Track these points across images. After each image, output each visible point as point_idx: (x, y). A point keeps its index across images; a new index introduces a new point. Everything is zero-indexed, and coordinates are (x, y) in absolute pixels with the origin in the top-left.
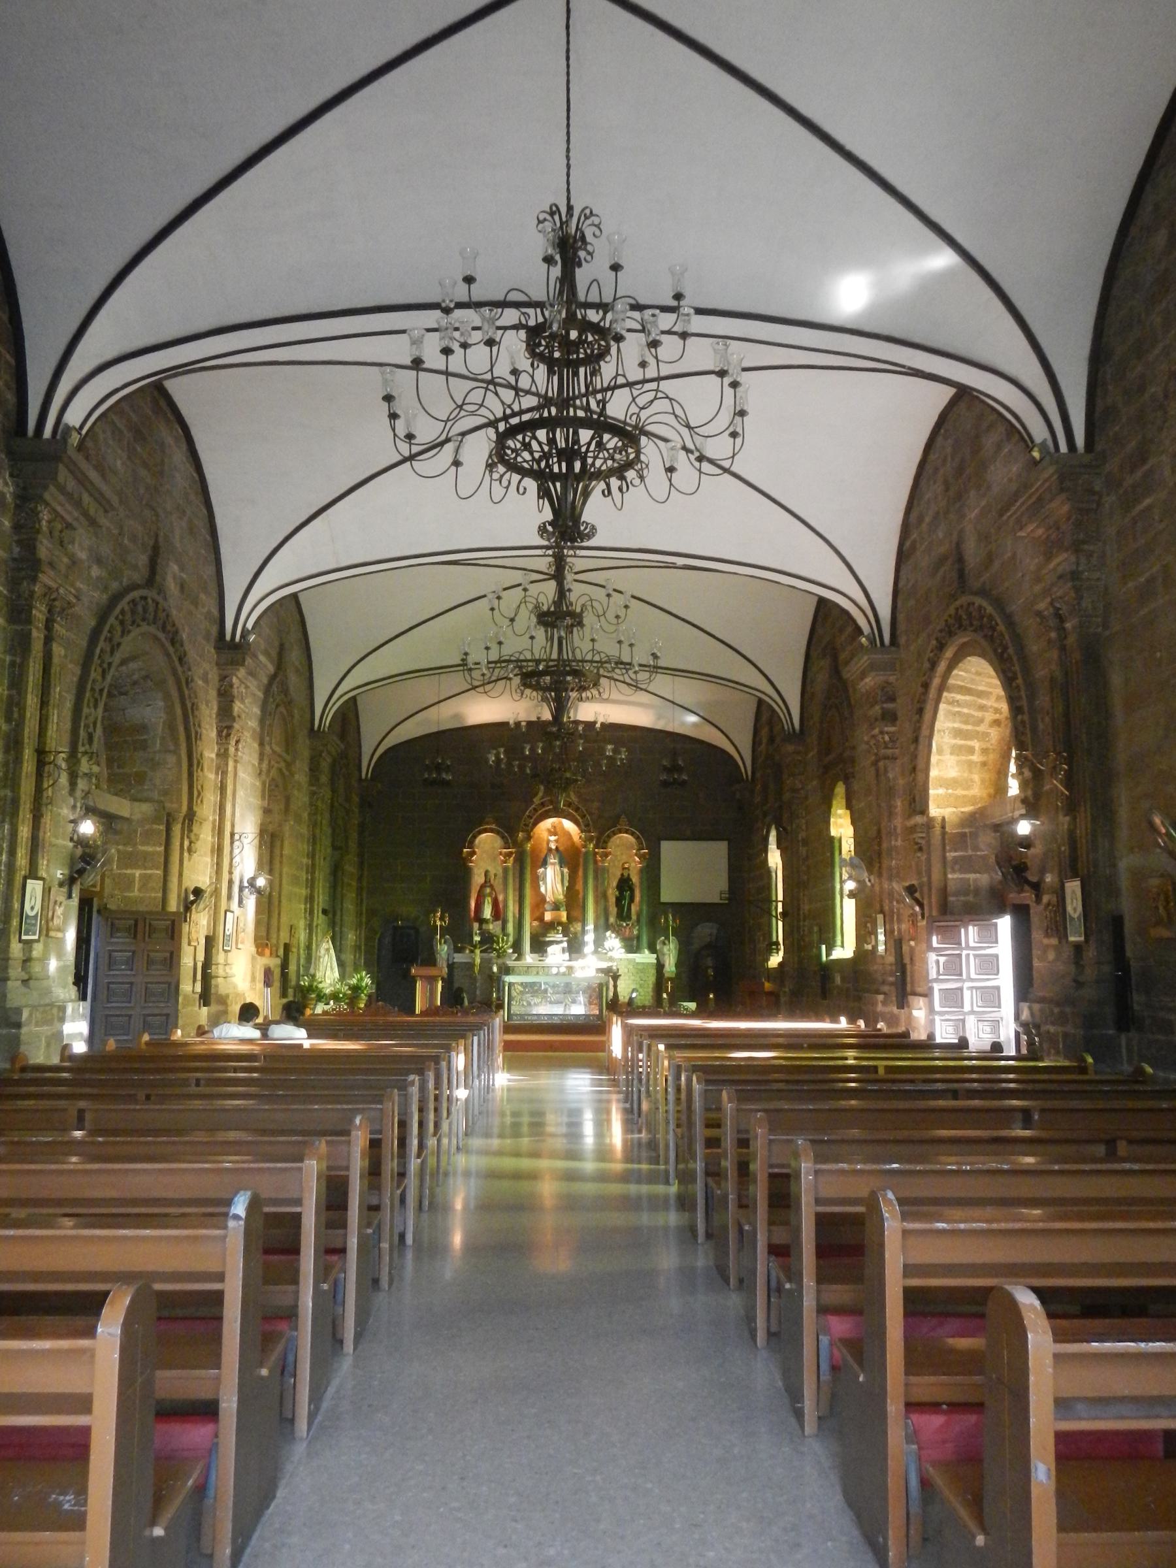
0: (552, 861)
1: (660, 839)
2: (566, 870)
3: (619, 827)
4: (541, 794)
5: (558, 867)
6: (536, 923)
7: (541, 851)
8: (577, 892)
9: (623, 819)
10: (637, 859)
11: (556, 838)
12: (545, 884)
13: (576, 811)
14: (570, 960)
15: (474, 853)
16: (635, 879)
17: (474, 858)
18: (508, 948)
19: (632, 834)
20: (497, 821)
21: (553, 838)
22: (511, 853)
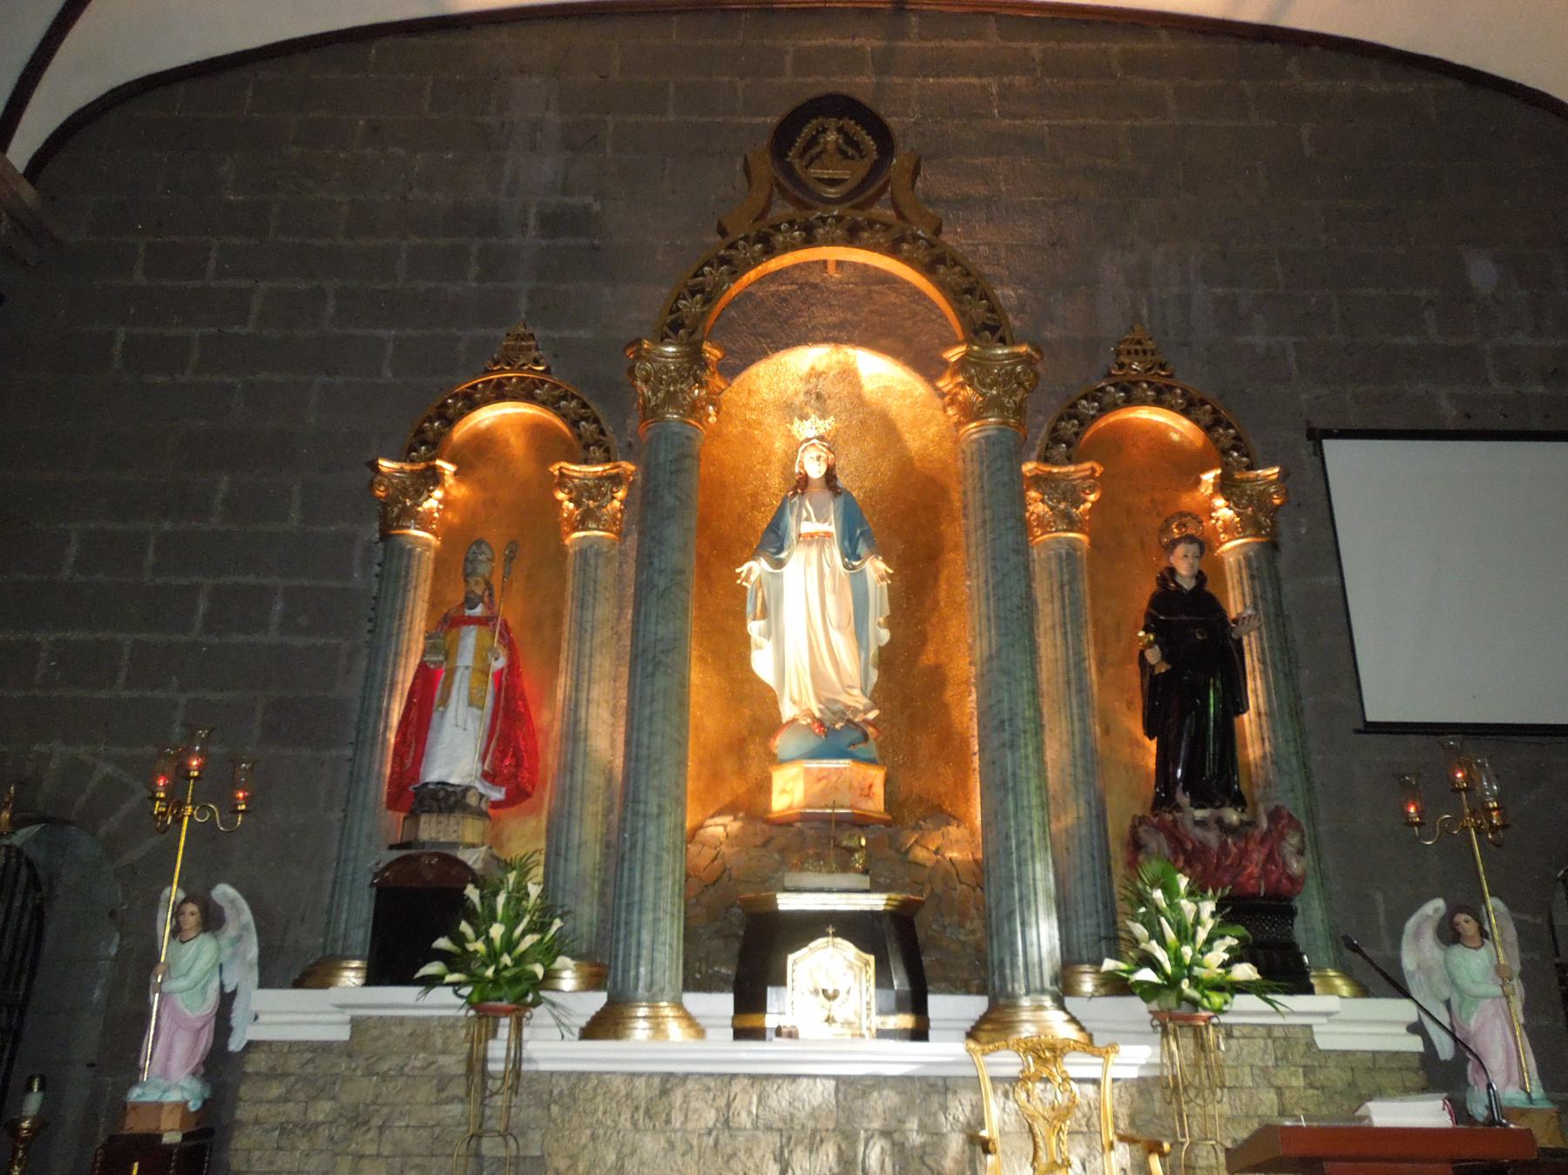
0: (806, 527)
1: (1317, 436)
2: (875, 568)
5: (834, 554)
6: (720, 828)
7: (755, 503)
8: (937, 678)
10: (1224, 511)
11: (825, 426)
12: (774, 632)
14: (919, 1033)
15: (435, 478)
17: (431, 503)
18: (548, 953)
21: (807, 428)
22: (616, 480)
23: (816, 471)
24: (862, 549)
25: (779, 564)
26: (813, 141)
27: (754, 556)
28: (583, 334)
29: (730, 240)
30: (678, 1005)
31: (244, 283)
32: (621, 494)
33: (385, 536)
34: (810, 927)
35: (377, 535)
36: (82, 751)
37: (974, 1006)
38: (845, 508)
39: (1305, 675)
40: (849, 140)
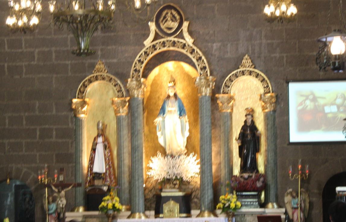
1: (288, 83)
2: (186, 119)
3: (241, 69)
4: (152, 36)
9: (246, 61)
13: (191, 53)
15: (84, 103)
16: (260, 126)
17: (85, 109)
19: (257, 76)
20: (110, 67)
23: (172, 94)
24: (182, 113)
25: (164, 118)
26: (165, 17)
27: (158, 116)
28: (115, 61)
29: (146, 48)
30: (144, 213)
31: (32, 50)
32: (127, 104)
33: (75, 116)
34: (168, 198)
35: (73, 115)
36: (19, 166)
37: (198, 212)
38: (179, 103)
39: (278, 141)
40: (174, 16)
